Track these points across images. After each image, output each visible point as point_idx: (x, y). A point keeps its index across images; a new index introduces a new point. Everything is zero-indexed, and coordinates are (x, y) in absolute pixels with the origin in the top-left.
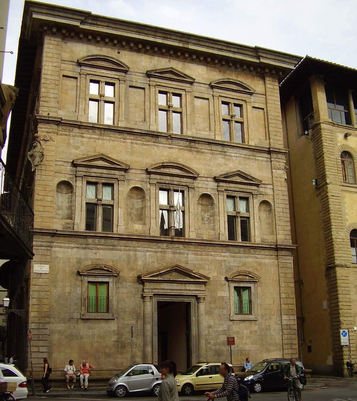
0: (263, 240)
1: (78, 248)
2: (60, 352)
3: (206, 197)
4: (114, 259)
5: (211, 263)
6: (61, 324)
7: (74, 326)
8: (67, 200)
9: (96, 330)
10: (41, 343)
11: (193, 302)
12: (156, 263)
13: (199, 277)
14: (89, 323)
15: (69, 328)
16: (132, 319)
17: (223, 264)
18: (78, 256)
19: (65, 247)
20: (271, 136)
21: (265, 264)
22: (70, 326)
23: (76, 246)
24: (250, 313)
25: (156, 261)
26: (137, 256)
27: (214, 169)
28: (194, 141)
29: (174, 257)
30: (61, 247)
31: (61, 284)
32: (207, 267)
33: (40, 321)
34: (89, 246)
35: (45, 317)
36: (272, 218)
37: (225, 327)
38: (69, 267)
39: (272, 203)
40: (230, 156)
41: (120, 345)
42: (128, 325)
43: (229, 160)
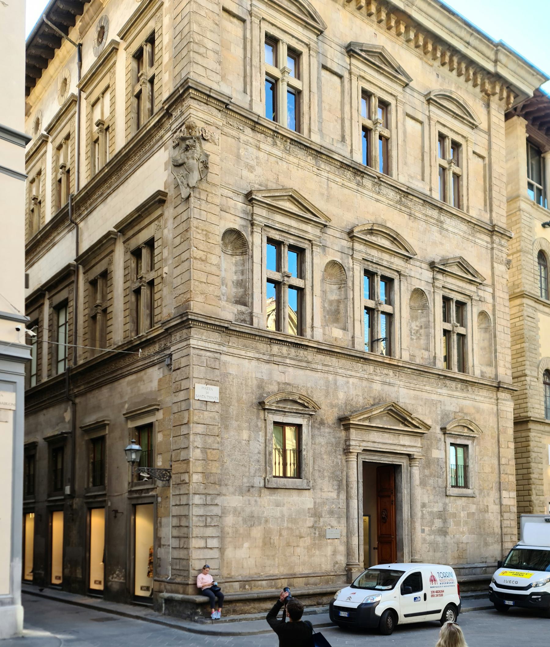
0: (483, 374)
1: (258, 359)
2: (235, 548)
3: (418, 293)
4: (309, 385)
5: (425, 404)
6: (237, 497)
7: (256, 501)
8: (234, 269)
9: (285, 509)
10: (210, 532)
11: (405, 464)
12: (361, 398)
13: (417, 425)
14: (276, 495)
15: (249, 504)
16: (332, 490)
17: (439, 405)
18: (259, 376)
19: (240, 357)
20: (495, 208)
22: (249, 500)
23: (257, 355)
24: (466, 486)
25: (361, 394)
26: (338, 384)
28: (407, 194)
29: (383, 390)
30: (233, 355)
31: (234, 424)
33: (206, 491)
34: (275, 359)
35: (215, 483)
36: (490, 339)
37: (437, 508)
38: (247, 393)
39: (491, 317)
40: (447, 230)
41: (317, 533)
42: (327, 499)
43: (445, 237)
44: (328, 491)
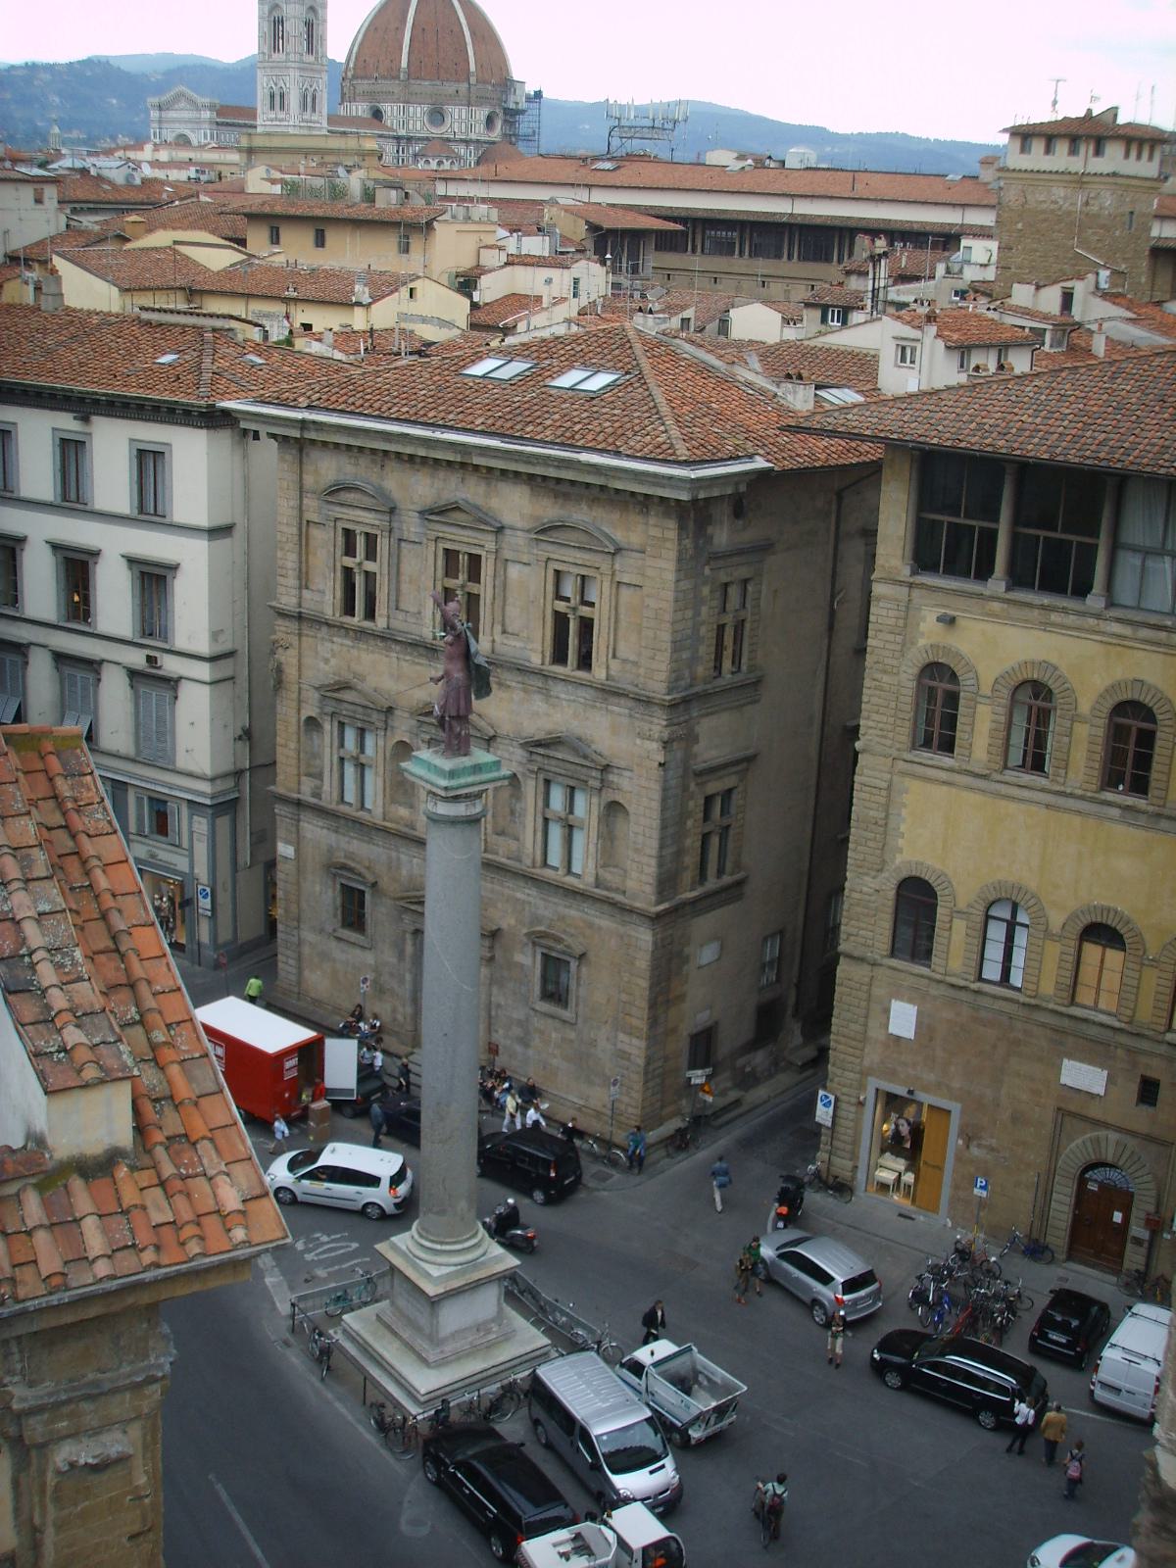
21: (600, 928)
32: (499, 905)
43: (554, 706)
44: (389, 956)
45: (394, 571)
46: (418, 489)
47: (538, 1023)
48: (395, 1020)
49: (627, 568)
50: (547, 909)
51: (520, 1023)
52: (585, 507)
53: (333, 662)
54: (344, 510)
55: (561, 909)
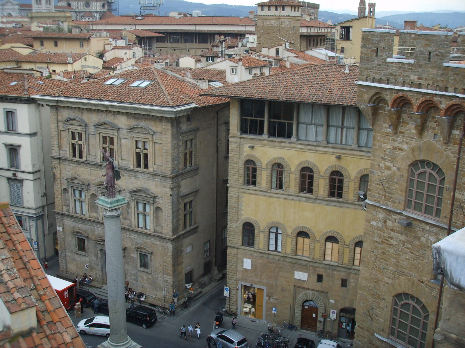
17: (134, 240)
21: (156, 244)
27: (130, 186)
32: (126, 240)
43: (138, 180)
44: (94, 258)
45: (87, 143)
46: (93, 119)
47: (140, 274)
48: (97, 277)
49: (157, 138)
50: (140, 240)
51: (134, 274)
52: (143, 121)
53: (71, 171)
54: (71, 126)
55: (144, 240)
